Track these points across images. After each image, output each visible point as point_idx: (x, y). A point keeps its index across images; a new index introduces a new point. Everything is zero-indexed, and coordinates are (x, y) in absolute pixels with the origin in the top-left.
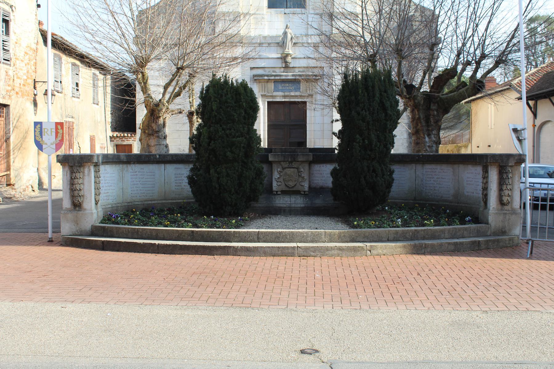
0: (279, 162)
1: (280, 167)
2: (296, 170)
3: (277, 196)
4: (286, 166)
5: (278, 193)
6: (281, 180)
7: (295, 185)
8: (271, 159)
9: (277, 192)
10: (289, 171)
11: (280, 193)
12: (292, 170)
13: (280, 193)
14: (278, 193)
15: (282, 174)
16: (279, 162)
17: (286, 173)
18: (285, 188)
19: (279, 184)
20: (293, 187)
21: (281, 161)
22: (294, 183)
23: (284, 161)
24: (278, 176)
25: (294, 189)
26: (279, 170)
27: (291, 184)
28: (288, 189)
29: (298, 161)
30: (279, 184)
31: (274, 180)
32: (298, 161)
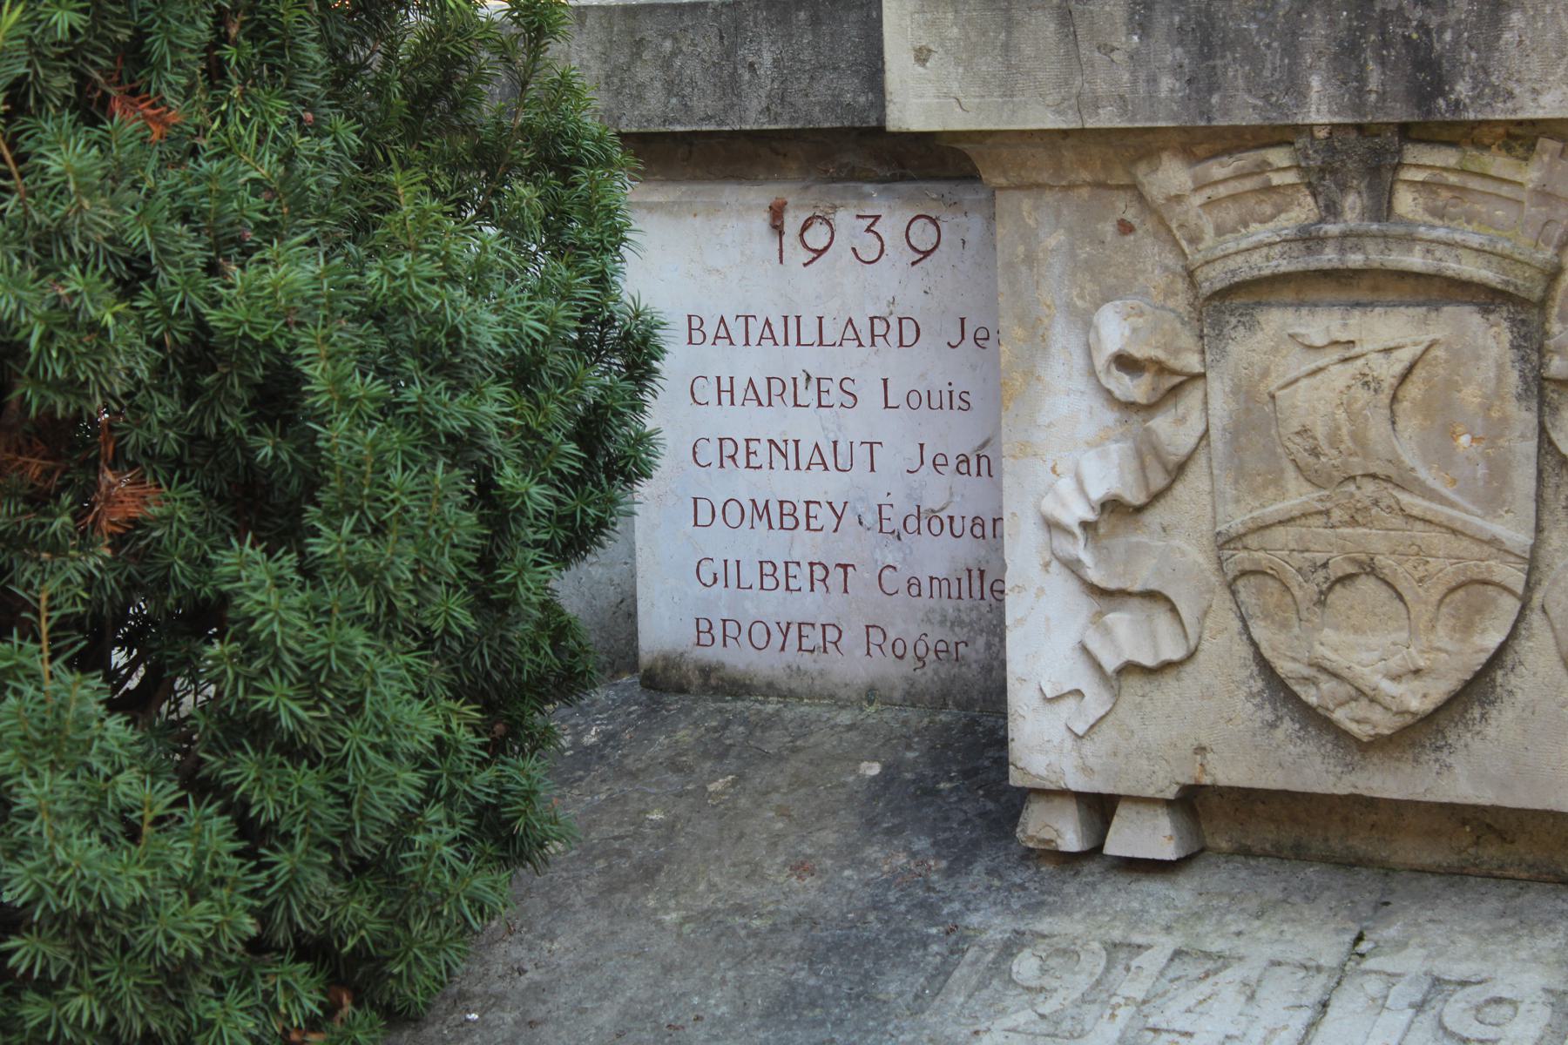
0: (1108, 156)
1: (1154, 261)
2: (1488, 340)
3: (1082, 921)
4: (1260, 243)
5: (1125, 839)
6: (1175, 549)
7: (1477, 689)
8: (917, 101)
9: (1100, 809)
10: (1316, 365)
11: (1152, 836)
12: (1391, 331)
13: (1152, 836)
14: (1125, 839)
15: (1176, 430)
16: (1108, 156)
17: (1257, 412)
18: (1255, 755)
19: (1130, 637)
20: (1421, 733)
21: (1137, 145)
22: (1455, 655)
23: (1202, 142)
24: (1107, 474)
25: (1464, 776)
26: (1114, 330)
27: (1382, 658)
28: (1317, 772)
29: (1521, 137)
30: (1130, 637)
31: (1024, 553)
32: (1521, 137)
